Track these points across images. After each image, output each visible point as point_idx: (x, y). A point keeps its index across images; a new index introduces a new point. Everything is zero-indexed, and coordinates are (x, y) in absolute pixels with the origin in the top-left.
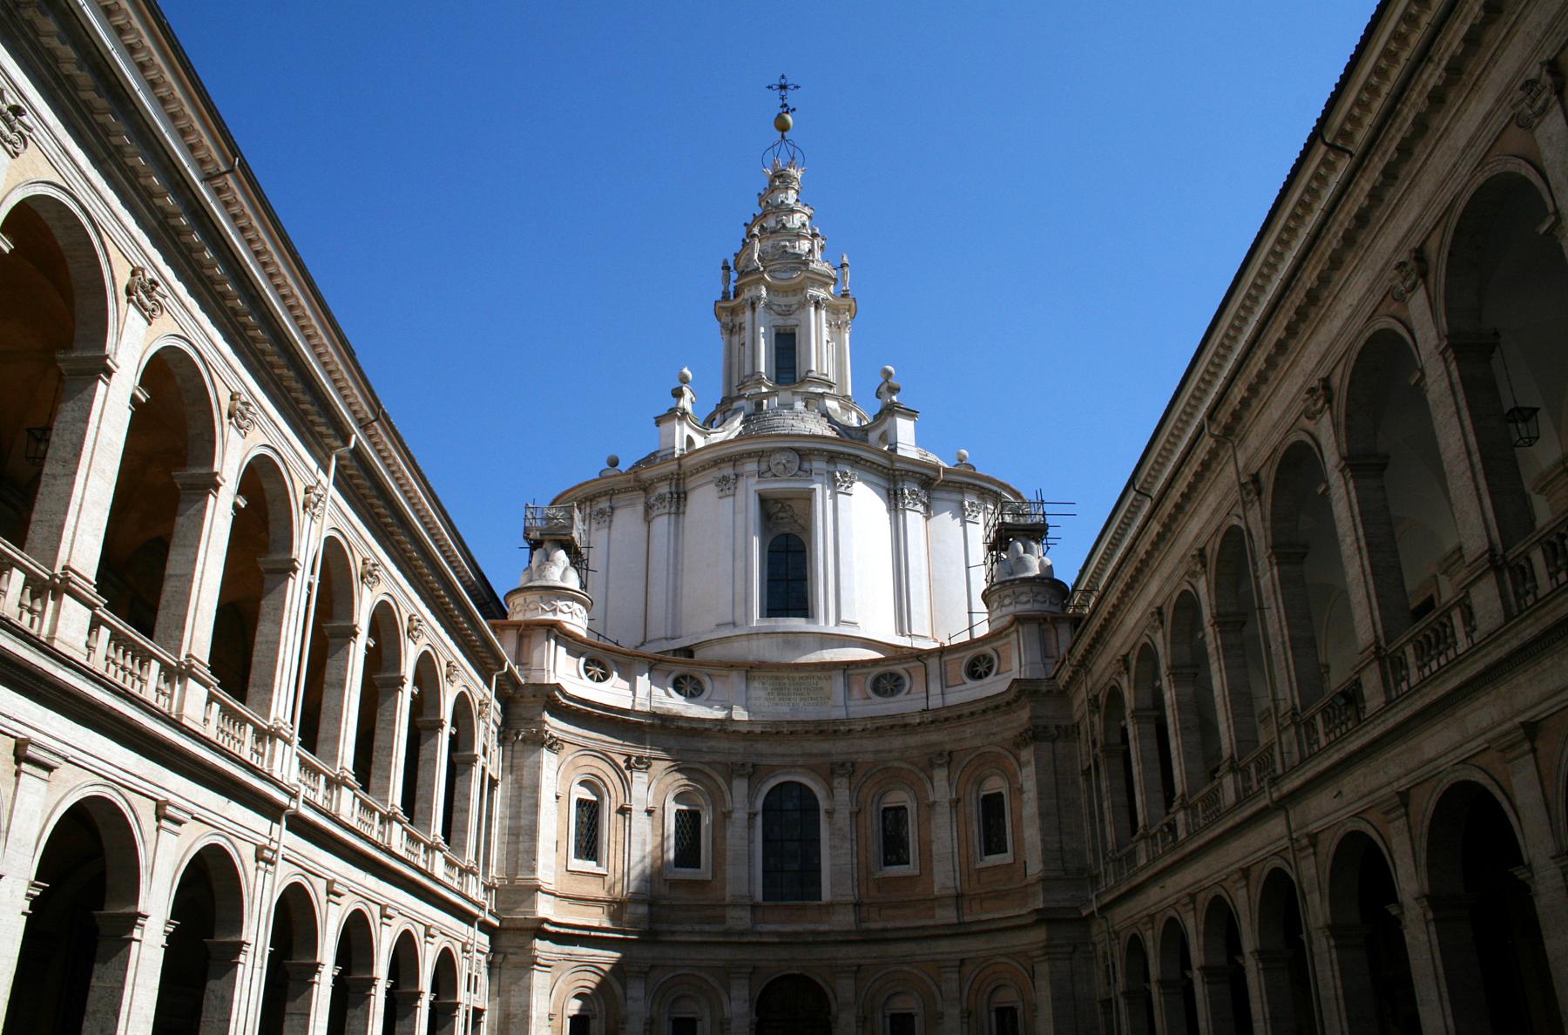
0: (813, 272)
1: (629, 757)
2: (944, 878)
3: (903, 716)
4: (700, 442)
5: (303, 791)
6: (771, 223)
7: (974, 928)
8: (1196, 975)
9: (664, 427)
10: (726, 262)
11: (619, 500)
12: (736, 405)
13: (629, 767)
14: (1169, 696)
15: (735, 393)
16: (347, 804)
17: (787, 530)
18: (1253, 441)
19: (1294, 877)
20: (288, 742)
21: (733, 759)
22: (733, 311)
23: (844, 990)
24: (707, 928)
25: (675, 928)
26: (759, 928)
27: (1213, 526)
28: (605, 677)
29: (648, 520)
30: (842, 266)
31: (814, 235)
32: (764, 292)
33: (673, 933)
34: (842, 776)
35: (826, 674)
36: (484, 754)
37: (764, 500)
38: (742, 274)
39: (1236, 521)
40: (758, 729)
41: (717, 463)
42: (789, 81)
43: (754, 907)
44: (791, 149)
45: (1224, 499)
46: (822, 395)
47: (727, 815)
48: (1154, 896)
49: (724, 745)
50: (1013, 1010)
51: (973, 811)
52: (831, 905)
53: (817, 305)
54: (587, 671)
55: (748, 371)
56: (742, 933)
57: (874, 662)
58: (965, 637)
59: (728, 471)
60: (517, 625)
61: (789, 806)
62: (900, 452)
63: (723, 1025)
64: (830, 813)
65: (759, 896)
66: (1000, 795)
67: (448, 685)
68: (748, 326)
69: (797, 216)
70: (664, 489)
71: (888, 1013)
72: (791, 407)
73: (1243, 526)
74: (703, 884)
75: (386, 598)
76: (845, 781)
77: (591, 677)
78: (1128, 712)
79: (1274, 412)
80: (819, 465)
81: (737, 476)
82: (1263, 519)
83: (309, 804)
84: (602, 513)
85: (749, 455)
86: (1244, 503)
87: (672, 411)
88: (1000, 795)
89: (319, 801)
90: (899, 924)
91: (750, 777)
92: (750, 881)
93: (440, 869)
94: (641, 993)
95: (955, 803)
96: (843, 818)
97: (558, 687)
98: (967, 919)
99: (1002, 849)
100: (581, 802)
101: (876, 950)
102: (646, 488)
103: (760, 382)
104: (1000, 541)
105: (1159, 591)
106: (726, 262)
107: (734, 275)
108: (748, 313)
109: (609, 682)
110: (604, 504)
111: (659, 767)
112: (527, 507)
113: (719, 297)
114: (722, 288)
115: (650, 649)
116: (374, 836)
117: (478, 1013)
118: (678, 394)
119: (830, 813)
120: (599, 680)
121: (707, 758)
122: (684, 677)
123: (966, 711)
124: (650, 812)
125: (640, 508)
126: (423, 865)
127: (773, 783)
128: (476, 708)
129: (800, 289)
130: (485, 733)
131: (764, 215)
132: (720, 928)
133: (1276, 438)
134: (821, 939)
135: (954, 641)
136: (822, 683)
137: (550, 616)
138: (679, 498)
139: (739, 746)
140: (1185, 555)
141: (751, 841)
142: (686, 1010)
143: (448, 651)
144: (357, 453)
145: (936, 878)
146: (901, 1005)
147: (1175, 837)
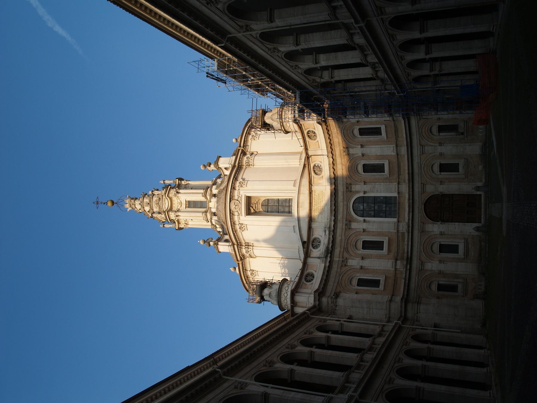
1: (342, 266)
2: (389, 150)
3: (329, 164)
5: (350, 393)
6: (147, 209)
7: (409, 140)
8: (428, 57)
13: (345, 265)
14: (323, 63)
15: (210, 223)
16: (356, 376)
17: (260, 205)
18: (228, 28)
19: (393, 16)
20: (331, 398)
21: (344, 227)
23: (431, 189)
24: (406, 239)
25: (406, 251)
26: (407, 220)
27: (260, 44)
28: (312, 276)
29: (256, 257)
33: (408, 252)
34: (351, 188)
35: (313, 192)
36: (339, 321)
37: (249, 213)
39: (258, 36)
40: (333, 218)
43: (398, 222)
44: (120, 201)
45: (249, 40)
47: (364, 230)
48: (399, 72)
49: (339, 231)
50: (439, 127)
51: (365, 138)
52: (399, 193)
54: (310, 281)
56: (409, 227)
57: (310, 174)
58: (301, 141)
59: (237, 227)
60: (292, 307)
61: (362, 207)
62: (233, 163)
63: (442, 234)
64: (365, 192)
65: (395, 220)
66: (360, 129)
67: (314, 334)
68: (185, 218)
71: (439, 173)
73: (260, 32)
74: (389, 240)
75: (279, 358)
76: (353, 187)
77: (312, 280)
78: (330, 80)
79: (216, 18)
80: (236, 193)
82: (257, 24)
83: (355, 391)
84: (252, 274)
86: (251, 31)
88: (360, 129)
89: (355, 386)
90: (407, 168)
91: (350, 221)
92: (389, 223)
93: (382, 340)
94: (430, 264)
95: (362, 146)
96: (366, 188)
97: (315, 292)
98: (405, 143)
99: (380, 129)
100: (358, 285)
101: (416, 177)
102: (243, 258)
104: (266, 126)
105: (284, 66)
108: (180, 218)
109: (314, 272)
110: (249, 273)
111: (346, 255)
112: (248, 302)
115: (302, 256)
116: (368, 364)
117: (435, 326)
119: (365, 192)
120: (313, 277)
121: (343, 237)
122: (313, 245)
123: (328, 141)
124: (363, 258)
125: (251, 259)
126: (380, 346)
127: (353, 213)
128: (321, 324)
130: (332, 322)
132: (406, 234)
133: (226, 18)
134: (411, 197)
135: (302, 144)
136: (317, 194)
137: (289, 293)
138: (248, 245)
139: (340, 225)
140: (271, 56)
141: (374, 222)
142: (436, 248)
143: (300, 333)
144: (221, 367)
145: (390, 154)
146: (436, 168)
147: (377, 63)
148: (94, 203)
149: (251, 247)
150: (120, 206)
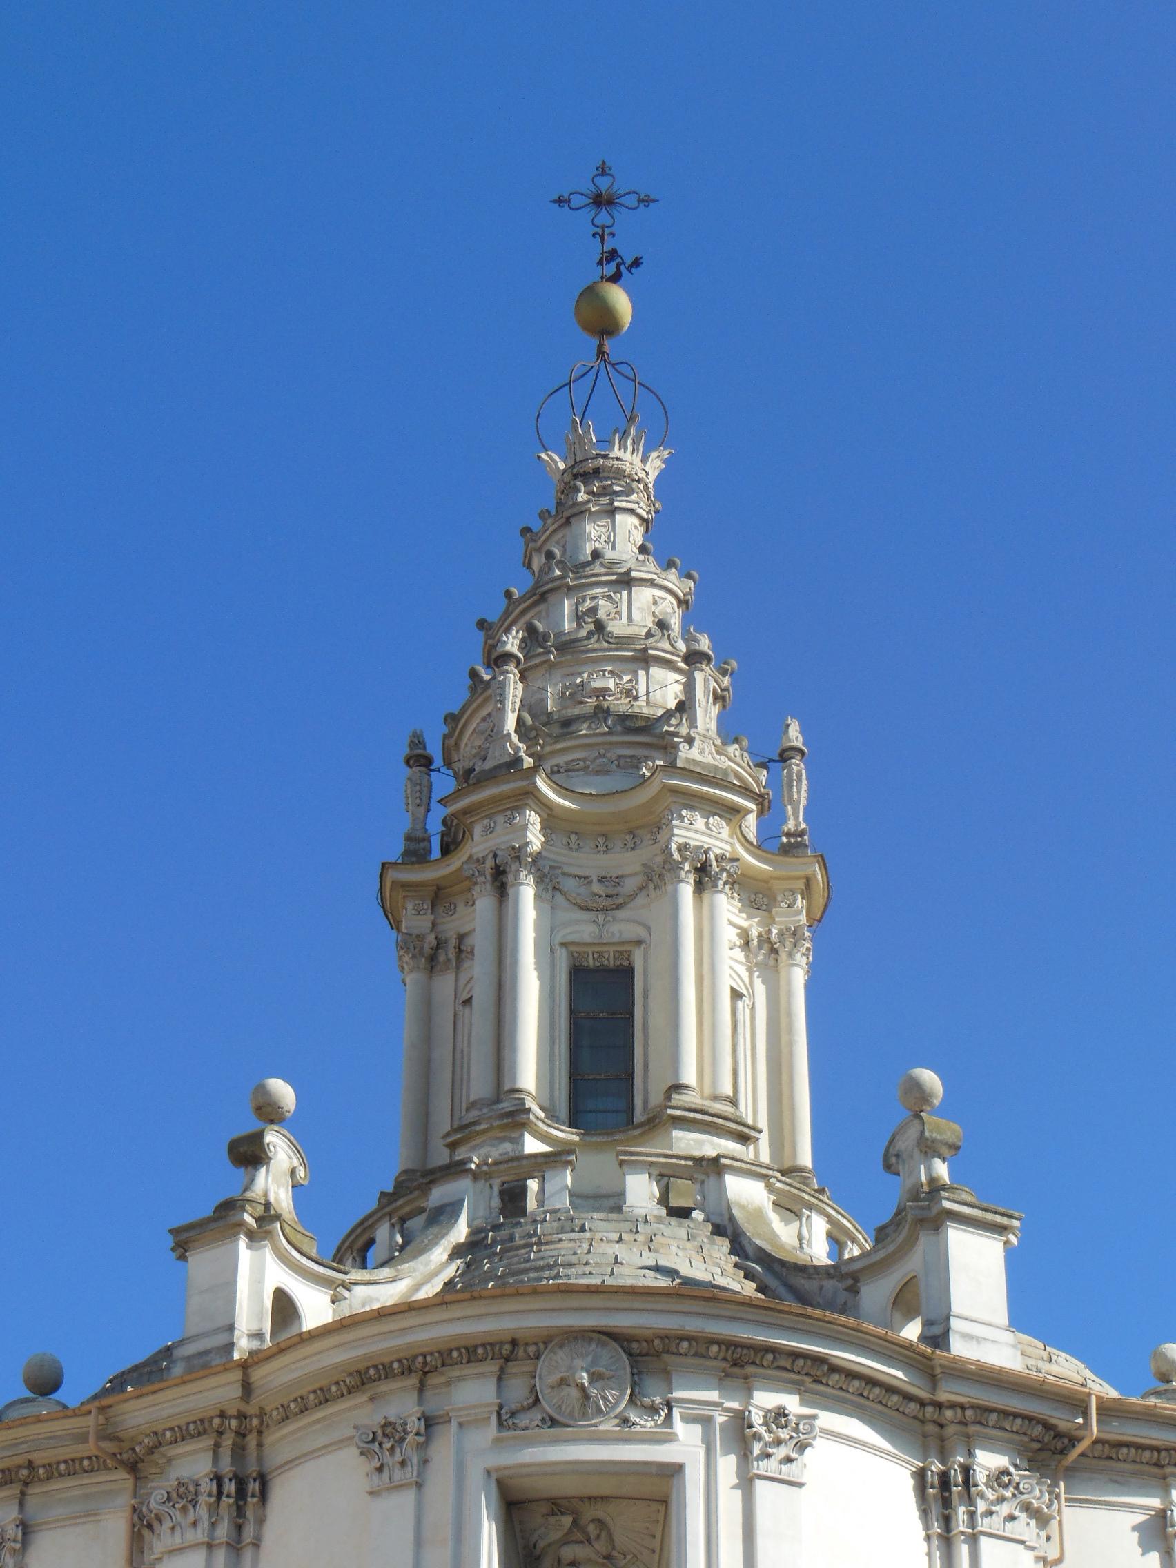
0: (687, 773)
4: (316, 1308)
9: (201, 1262)
10: (417, 741)
11: (48, 1500)
12: (439, 1194)
15: (441, 1157)
22: (438, 897)
30: (784, 756)
31: (694, 658)
32: (535, 840)
38: (469, 779)
41: (364, 1378)
42: (620, 183)
46: (714, 1167)
53: (704, 876)
55: (479, 1086)
59: (401, 1405)
68: (482, 942)
69: (643, 595)
70: (194, 1464)
72: (613, 1202)
81: (430, 1423)
85: (470, 1353)
87: (229, 1207)
103: (516, 1120)
106: (417, 741)
107: (443, 783)
108: (484, 903)
113: (395, 850)
114: (404, 824)
118: (249, 1154)
129: (649, 826)
131: (542, 595)
148: (603, 170)
149: (223, 1531)
150: (581, 390)
